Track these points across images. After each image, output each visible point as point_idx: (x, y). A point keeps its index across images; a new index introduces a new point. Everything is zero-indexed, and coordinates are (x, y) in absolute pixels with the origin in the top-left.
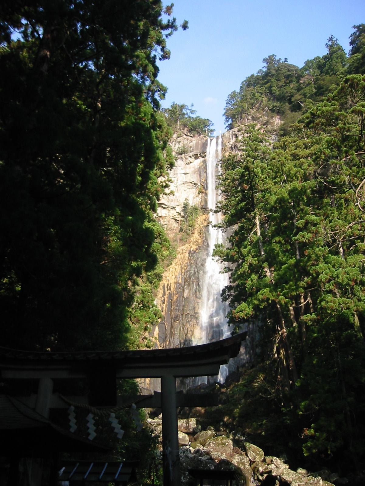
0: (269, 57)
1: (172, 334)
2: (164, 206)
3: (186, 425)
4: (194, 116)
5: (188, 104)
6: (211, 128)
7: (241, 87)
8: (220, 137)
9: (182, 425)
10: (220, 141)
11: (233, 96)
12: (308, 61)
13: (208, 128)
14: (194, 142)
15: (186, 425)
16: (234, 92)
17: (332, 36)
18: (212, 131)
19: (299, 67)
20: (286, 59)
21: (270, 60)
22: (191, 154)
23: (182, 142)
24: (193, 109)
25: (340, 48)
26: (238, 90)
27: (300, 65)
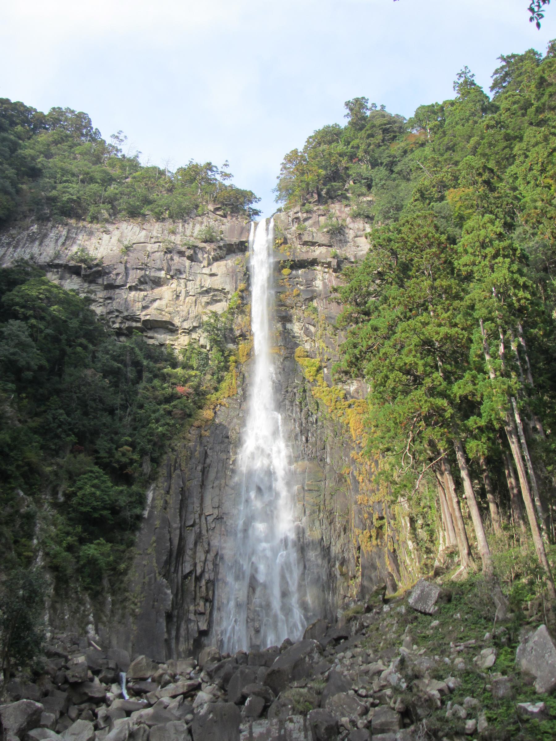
0: (357, 100)
1: (181, 551)
2: (171, 327)
3: (280, 730)
4: (227, 183)
5: (217, 162)
6: (254, 206)
7: (306, 148)
8: (272, 220)
9: (269, 731)
10: (272, 225)
11: (293, 157)
12: (423, 107)
13: (250, 206)
14: (228, 225)
15: (280, 732)
16: (295, 152)
17: (466, 67)
18: (256, 213)
19: (405, 119)
20: (383, 107)
21: (357, 106)
22: (222, 244)
23: (205, 224)
24: (227, 171)
25: (479, 90)
26: (301, 149)
27: (408, 113)
